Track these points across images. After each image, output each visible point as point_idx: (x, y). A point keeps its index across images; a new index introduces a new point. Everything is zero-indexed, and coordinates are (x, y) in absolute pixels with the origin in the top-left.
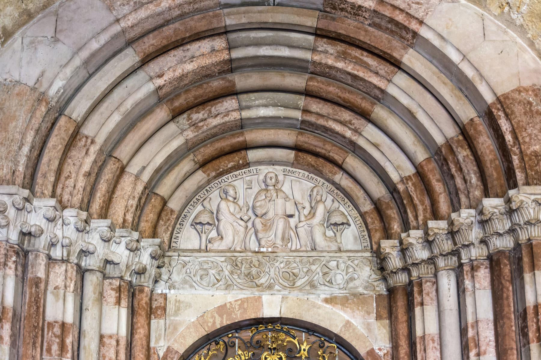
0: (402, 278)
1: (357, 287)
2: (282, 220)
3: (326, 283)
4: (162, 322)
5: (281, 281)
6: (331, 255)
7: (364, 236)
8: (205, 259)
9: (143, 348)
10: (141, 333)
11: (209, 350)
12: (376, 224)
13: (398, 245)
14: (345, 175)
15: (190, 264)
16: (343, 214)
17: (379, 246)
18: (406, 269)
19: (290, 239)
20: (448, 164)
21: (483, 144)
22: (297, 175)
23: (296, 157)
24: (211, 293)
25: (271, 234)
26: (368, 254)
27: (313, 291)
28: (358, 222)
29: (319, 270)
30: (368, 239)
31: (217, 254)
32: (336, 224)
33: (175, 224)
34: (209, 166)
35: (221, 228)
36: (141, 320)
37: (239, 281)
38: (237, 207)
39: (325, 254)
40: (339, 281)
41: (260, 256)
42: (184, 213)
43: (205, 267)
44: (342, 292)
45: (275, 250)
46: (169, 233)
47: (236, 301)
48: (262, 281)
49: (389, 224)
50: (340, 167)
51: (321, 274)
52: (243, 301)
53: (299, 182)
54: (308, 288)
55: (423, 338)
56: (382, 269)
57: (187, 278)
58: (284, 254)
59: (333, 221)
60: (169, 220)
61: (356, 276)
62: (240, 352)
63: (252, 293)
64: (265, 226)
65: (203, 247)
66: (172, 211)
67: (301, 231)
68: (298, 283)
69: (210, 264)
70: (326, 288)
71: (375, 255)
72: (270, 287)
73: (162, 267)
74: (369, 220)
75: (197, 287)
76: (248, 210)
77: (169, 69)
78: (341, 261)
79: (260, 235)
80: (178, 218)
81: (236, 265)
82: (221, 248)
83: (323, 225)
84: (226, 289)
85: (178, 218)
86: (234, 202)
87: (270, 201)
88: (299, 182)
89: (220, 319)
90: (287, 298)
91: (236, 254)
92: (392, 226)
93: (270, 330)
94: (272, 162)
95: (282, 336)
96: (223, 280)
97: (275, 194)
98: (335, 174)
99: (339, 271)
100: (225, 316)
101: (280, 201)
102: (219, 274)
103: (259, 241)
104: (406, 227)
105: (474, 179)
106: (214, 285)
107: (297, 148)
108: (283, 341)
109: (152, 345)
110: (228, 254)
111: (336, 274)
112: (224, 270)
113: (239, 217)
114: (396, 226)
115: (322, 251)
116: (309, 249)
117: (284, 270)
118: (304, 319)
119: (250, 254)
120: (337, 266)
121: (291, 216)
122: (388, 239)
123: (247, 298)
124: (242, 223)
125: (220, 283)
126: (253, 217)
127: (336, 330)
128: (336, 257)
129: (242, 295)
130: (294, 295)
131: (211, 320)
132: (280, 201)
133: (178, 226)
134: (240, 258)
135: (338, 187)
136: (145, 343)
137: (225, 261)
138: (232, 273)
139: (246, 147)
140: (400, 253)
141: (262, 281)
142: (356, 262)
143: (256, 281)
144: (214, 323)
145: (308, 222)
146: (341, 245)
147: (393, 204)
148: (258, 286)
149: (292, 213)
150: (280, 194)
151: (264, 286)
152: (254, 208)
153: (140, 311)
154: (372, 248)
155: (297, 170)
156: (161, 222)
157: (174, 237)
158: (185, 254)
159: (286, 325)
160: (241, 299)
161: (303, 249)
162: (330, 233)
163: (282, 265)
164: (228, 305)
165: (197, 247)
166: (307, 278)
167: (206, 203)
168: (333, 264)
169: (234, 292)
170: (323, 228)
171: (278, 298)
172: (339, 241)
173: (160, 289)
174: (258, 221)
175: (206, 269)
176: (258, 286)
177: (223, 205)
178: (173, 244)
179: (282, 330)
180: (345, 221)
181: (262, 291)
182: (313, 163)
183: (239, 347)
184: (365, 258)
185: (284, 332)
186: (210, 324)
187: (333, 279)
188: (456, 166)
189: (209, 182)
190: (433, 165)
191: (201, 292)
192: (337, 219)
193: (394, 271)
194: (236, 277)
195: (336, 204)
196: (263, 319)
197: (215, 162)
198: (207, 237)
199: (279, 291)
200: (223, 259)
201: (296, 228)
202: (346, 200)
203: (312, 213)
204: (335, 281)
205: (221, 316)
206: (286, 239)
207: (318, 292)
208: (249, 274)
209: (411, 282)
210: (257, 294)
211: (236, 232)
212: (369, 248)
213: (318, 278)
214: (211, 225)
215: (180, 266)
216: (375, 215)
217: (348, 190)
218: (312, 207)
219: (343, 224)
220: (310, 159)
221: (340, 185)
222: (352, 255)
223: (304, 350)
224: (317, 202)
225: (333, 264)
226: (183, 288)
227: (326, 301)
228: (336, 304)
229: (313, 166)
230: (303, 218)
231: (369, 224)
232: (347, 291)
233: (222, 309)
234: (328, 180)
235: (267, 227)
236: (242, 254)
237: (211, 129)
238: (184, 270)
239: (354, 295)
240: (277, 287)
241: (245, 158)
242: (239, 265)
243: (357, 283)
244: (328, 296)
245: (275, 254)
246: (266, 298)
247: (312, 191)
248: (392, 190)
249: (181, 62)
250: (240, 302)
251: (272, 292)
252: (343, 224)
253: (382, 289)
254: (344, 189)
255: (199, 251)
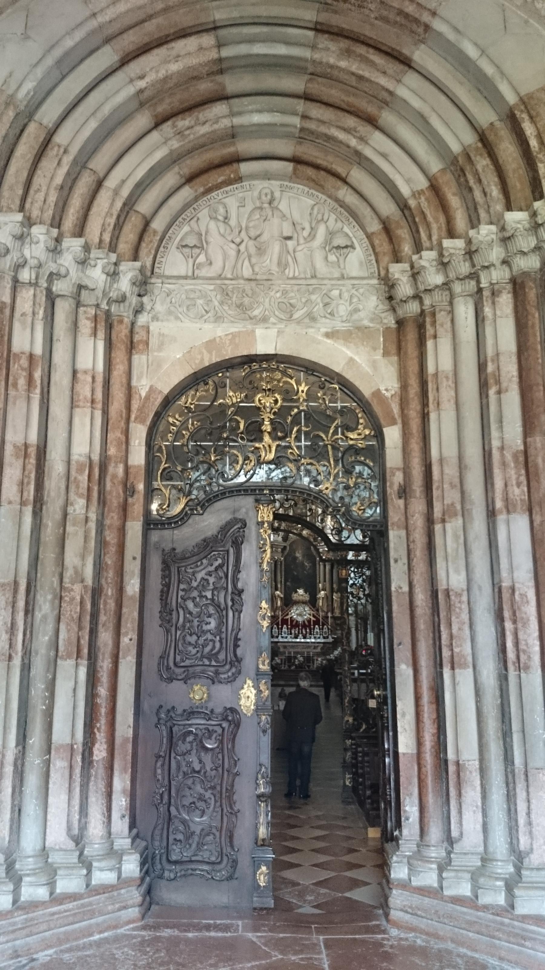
0: (413, 308)
1: (362, 320)
2: (278, 242)
3: (328, 316)
4: (144, 357)
5: (277, 313)
6: (333, 282)
7: (370, 261)
8: (192, 287)
9: (122, 386)
10: (119, 370)
11: (197, 390)
12: (384, 246)
13: (409, 269)
14: (350, 191)
15: (175, 293)
16: (347, 235)
17: (387, 271)
18: (417, 297)
19: (287, 265)
20: (465, 175)
21: (504, 151)
22: (295, 191)
23: (295, 170)
24: (198, 325)
25: (266, 258)
26: (375, 281)
27: (313, 324)
28: (364, 245)
29: (319, 300)
30: (375, 264)
31: (205, 282)
32: (338, 247)
33: (159, 247)
34: (198, 180)
35: (210, 251)
36: (120, 355)
37: (230, 312)
38: (228, 228)
39: (325, 282)
40: (342, 313)
41: (253, 284)
42: (168, 235)
43: (192, 296)
44: (345, 325)
45: (270, 277)
46: (152, 256)
47: (226, 335)
48: (256, 312)
49: (399, 246)
50: (344, 181)
51: (321, 305)
52: (234, 335)
53: (298, 199)
54: (307, 320)
55: (436, 375)
56: (390, 298)
57: (172, 309)
58: (280, 282)
59: (336, 242)
60: (151, 242)
61: (361, 307)
62: (231, 394)
63: (244, 327)
64: (259, 249)
65: (190, 274)
66: (155, 232)
67: (300, 256)
68: (296, 316)
69: (198, 294)
70: (327, 321)
71: (383, 282)
72: (264, 320)
73: (144, 295)
74: (377, 242)
75: (183, 319)
76: (240, 232)
77: (151, 69)
78: (344, 289)
79: (254, 260)
80: (161, 240)
81: (227, 294)
82: (209, 275)
83: (325, 248)
84: (215, 322)
85: (161, 240)
86: (224, 222)
87: (265, 220)
88: (298, 199)
89: (208, 355)
90: (283, 332)
91: (227, 282)
92: (402, 248)
93: (265, 369)
94: (267, 176)
95: (278, 375)
96: (212, 311)
97: (270, 213)
98: (338, 189)
99: (342, 302)
100: (214, 353)
101: (276, 221)
102: (208, 305)
103: (252, 266)
104: (418, 248)
105: (495, 192)
106: (202, 316)
107: (296, 160)
108: (279, 381)
109: (134, 383)
110: (218, 282)
111: (338, 305)
112: (214, 300)
113: (230, 239)
114: (407, 248)
115: (323, 279)
116: (309, 276)
117: (280, 300)
118: (303, 356)
119: (242, 282)
120: (340, 295)
121: (289, 238)
122: (397, 262)
123: (239, 332)
124: (233, 246)
125: (209, 314)
126: (246, 239)
127: (337, 369)
128: (339, 285)
129: (234, 329)
130: (291, 329)
131: (199, 357)
132: (276, 221)
133: (161, 249)
134: (231, 287)
135: (342, 204)
136: (124, 380)
137: (214, 290)
138: (222, 303)
139: (238, 159)
140: (411, 278)
141: (256, 312)
142: (361, 291)
143: (249, 312)
144: (202, 359)
145: (307, 245)
146: (344, 271)
147: (404, 223)
148: (251, 318)
149: (289, 234)
150: (276, 213)
151: (258, 318)
152: (247, 228)
153: (119, 345)
154: (379, 275)
155: (296, 185)
156: (143, 245)
157: (157, 261)
158: (170, 281)
159: (282, 363)
160: (232, 333)
161: (302, 276)
162: (332, 258)
163: (278, 295)
164: (218, 340)
165: (183, 273)
166: (305, 309)
167: (193, 222)
168: (336, 293)
169: (224, 325)
170: (324, 252)
171: (273, 332)
172: (342, 266)
173: (142, 319)
174: (251, 243)
175: (193, 299)
176: (251, 318)
177: (212, 225)
178: (156, 270)
179: (278, 369)
180: (349, 243)
181: (256, 324)
182: (314, 177)
183: (230, 388)
184: (372, 286)
185: (280, 371)
186: (197, 362)
187: (335, 310)
188: (474, 177)
189: (196, 199)
190: (449, 176)
191: (187, 324)
192: (340, 241)
193: (404, 299)
194: (226, 308)
195: (340, 224)
196: (256, 355)
197: (205, 177)
198: (195, 262)
199: (274, 324)
200: (212, 287)
201: (294, 251)
202: (351, 219)
203: (312, 236)
204: (338, 313)
205: (210, 352)
206: (282, 265)
207: (318, 325)
208: (241, 304)
209: (423, 312)
210: (250, 327)
211: (225, 257)
212: (377, 274)
213: (318, 309)
214: (199, 248)
215: (164, 295)
216: (384, 236)
217: (353, 207)
218: (312, 228)
219: (346, 247)
220: (310, 172)
221: (343, 202)
222: (356, 282)
223: (303, 391)
224: (318, 222)
225: (336, 293)
226: (168, 320)
227: (327, 335)
228: (338, 338)
229: (314, 181)
230: (302, 241)
231: (377, 247)
232: (350, 324)
233: (210, 344)
234: (330, 197)
235: (261, 251)
236: (233, 282)
237: (198, 138)
238: (168, 299)
239: (359, 328)
240: (272, 320)
241: (237, 171)
242: (230, 294)
243: (362, 314)
244: (329, 330)
245: (270, 282)
246: (259, 332)
247: (312, 209)
248: (402, 206)
249: (166, 62)
250: (230, 336)
251: (267, 325)
252: (346, 247)
253: (390, 321)
254: (349, 207)
255: (186, 278)
